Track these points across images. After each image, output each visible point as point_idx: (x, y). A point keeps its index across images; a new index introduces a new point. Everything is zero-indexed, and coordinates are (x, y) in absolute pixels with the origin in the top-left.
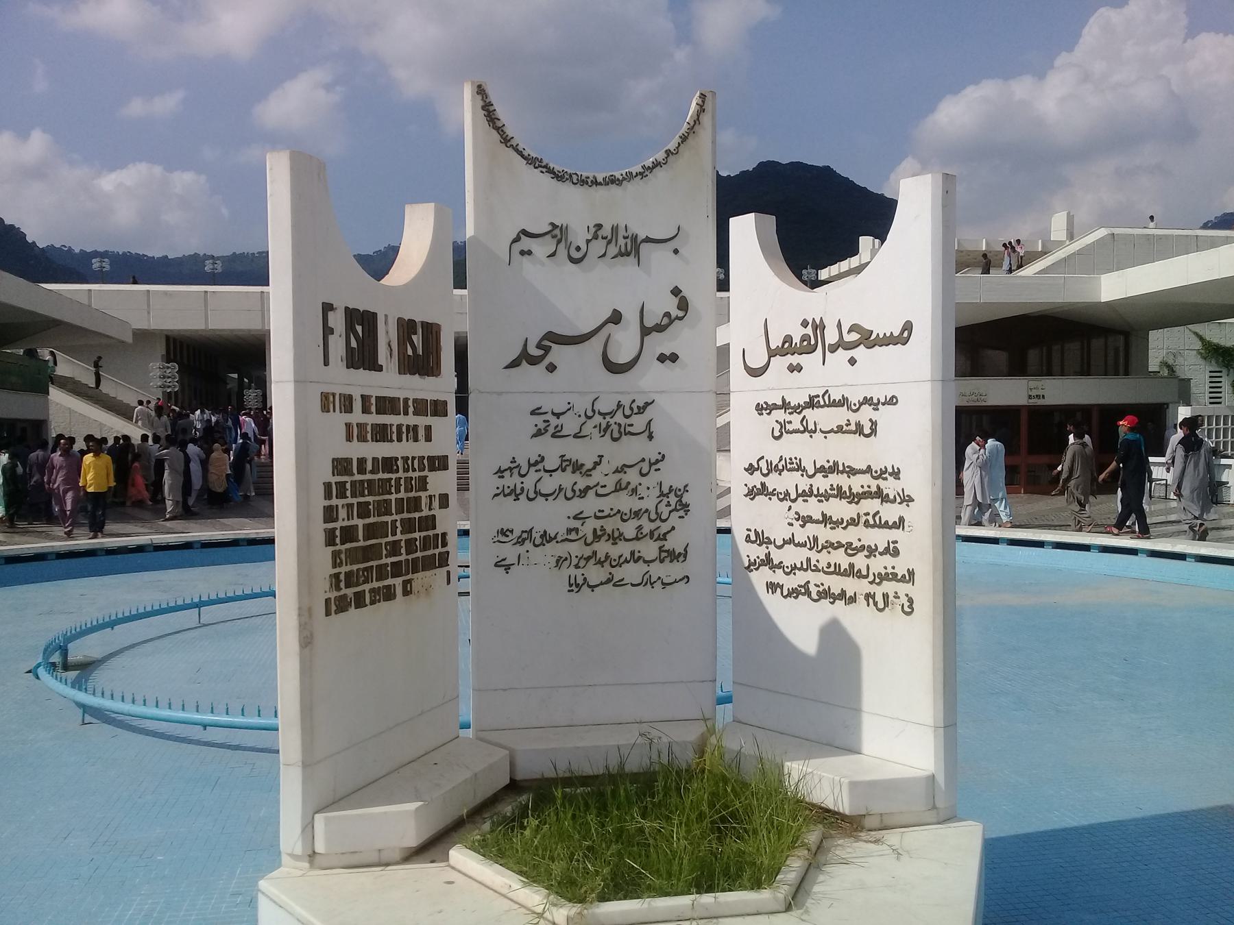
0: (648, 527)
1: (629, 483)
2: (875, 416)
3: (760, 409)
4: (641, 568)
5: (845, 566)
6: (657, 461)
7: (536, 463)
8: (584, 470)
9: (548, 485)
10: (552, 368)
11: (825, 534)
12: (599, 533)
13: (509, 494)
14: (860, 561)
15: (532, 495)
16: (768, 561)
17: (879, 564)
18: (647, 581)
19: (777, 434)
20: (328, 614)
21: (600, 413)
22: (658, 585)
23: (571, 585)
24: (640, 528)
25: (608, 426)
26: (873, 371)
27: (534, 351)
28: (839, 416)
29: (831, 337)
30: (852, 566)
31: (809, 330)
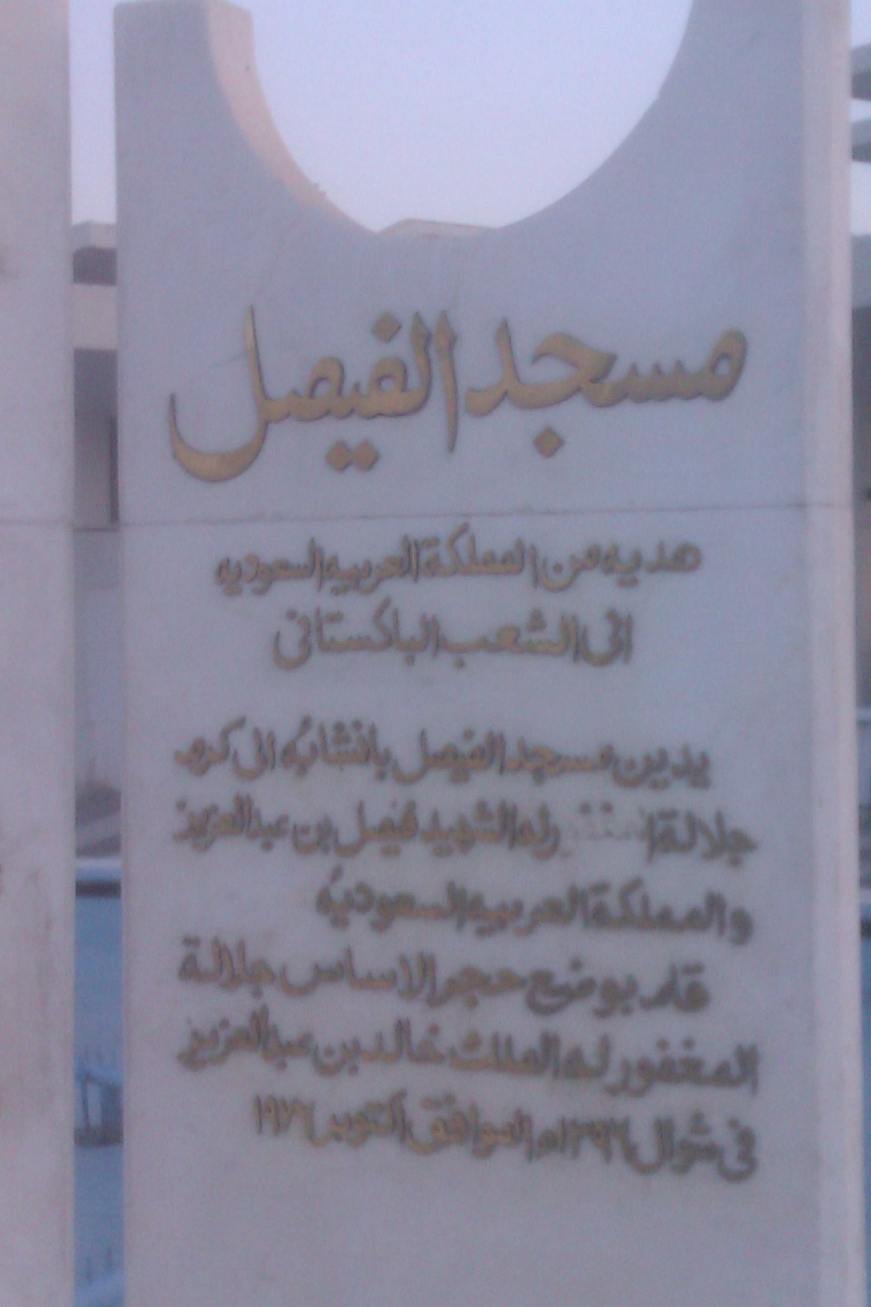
2: (624, 600)
3: (230, 576)
11: (457, 949)
14: (577, 1027)
16: (259, 1036)
17: (639, 1035)
26: (628, 472)
28: (506, 600)
29: (476, 364)
30: (550, 1042)
31: (401, 347)
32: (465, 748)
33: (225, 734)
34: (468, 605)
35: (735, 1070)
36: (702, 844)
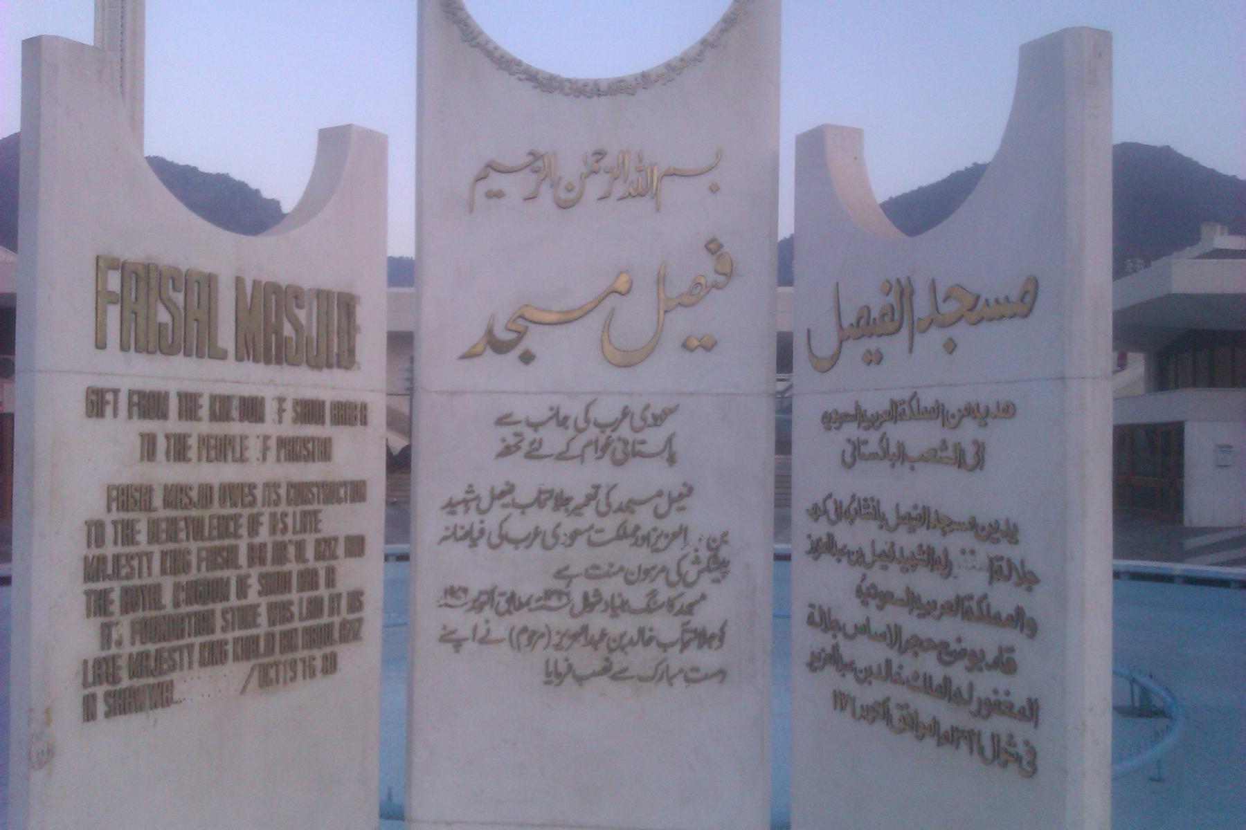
0: (664, 594)
1: (637, 528)
4: (653, 651)
5: (938, 680)
6: (681, 496)
7: (503, 494)
8: (571, 506)
9: (519, 526)
10: (527, 358)
11: (912, 625)
12: (592, 599)
13: (463, 538)
14: (959, 674)
15: (495, 540)
16: (833, 658)
17: (987, 684)
18: (663, 675)
19: (848, 460)
20: (89, 715)
21: (597, 425)
22: (679, 683)
23: (548, 674)
24: (653, 594)
25: (607, 445)
27: (503, 335)
29: (922, 306)
30: (947, 680)
31: (892, 299)
32: (914, 514)
33: (824, 502)
34: (917, 436)
35: (1028, 713)
36: (1015, 578)
